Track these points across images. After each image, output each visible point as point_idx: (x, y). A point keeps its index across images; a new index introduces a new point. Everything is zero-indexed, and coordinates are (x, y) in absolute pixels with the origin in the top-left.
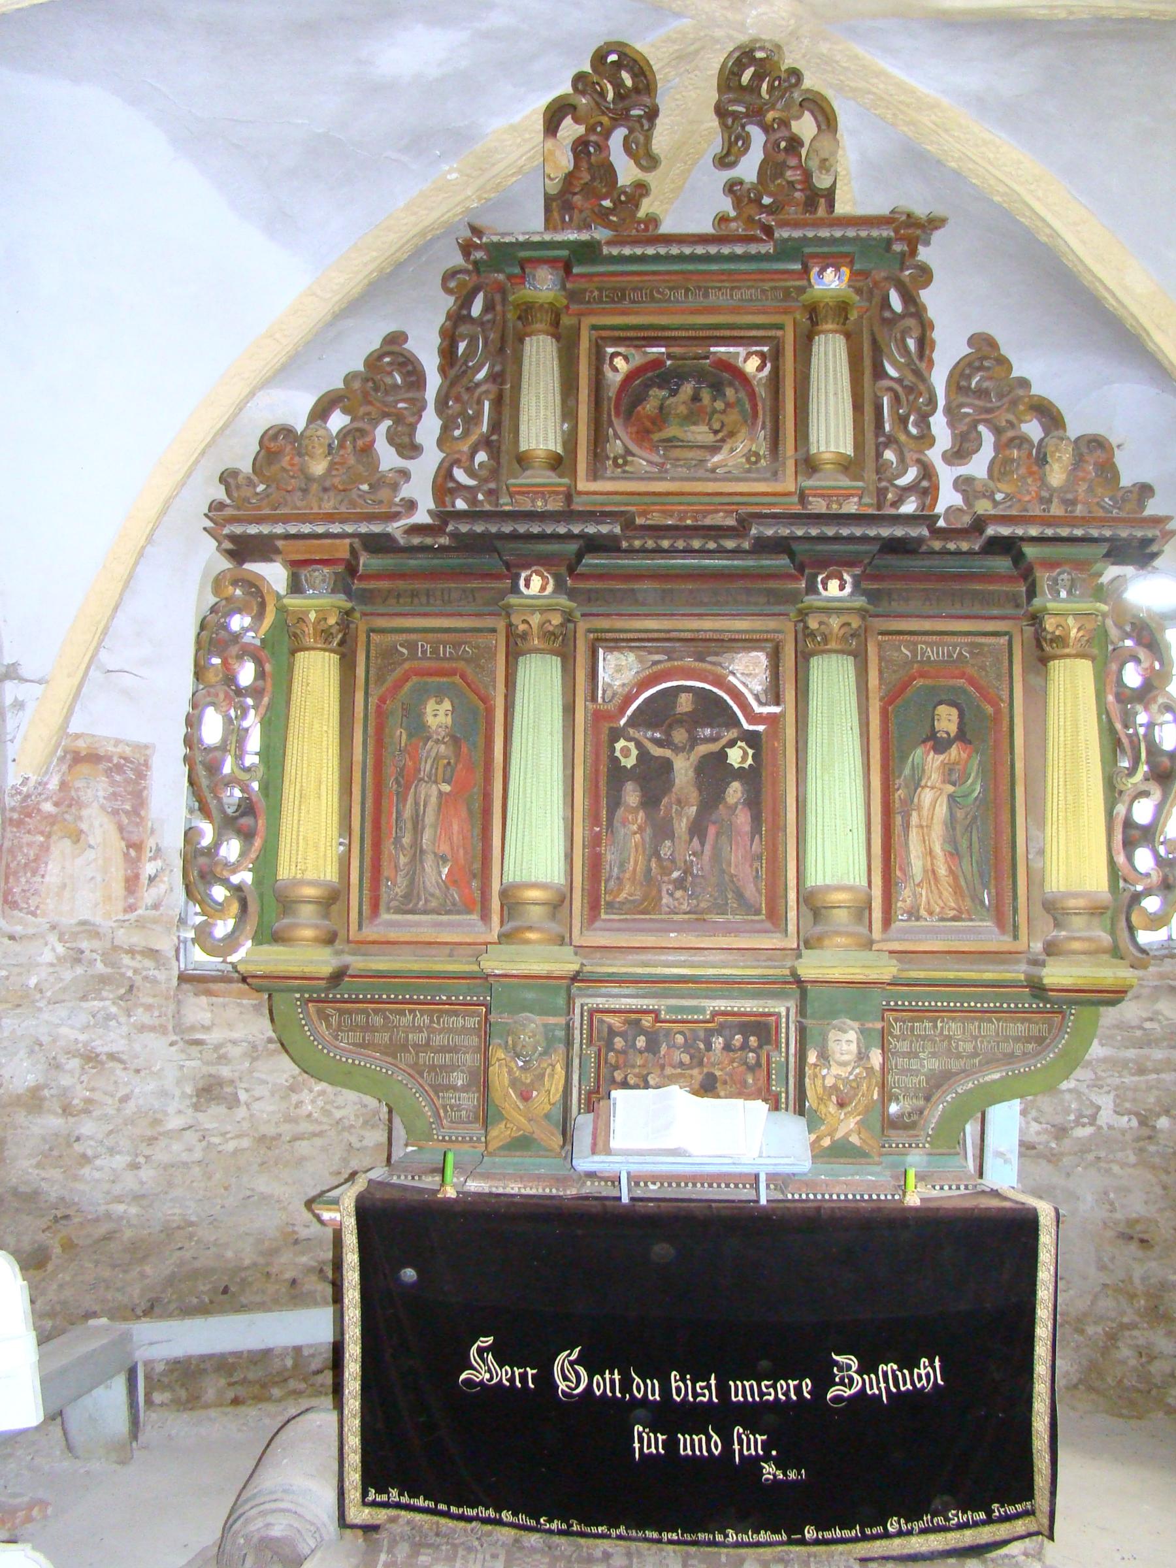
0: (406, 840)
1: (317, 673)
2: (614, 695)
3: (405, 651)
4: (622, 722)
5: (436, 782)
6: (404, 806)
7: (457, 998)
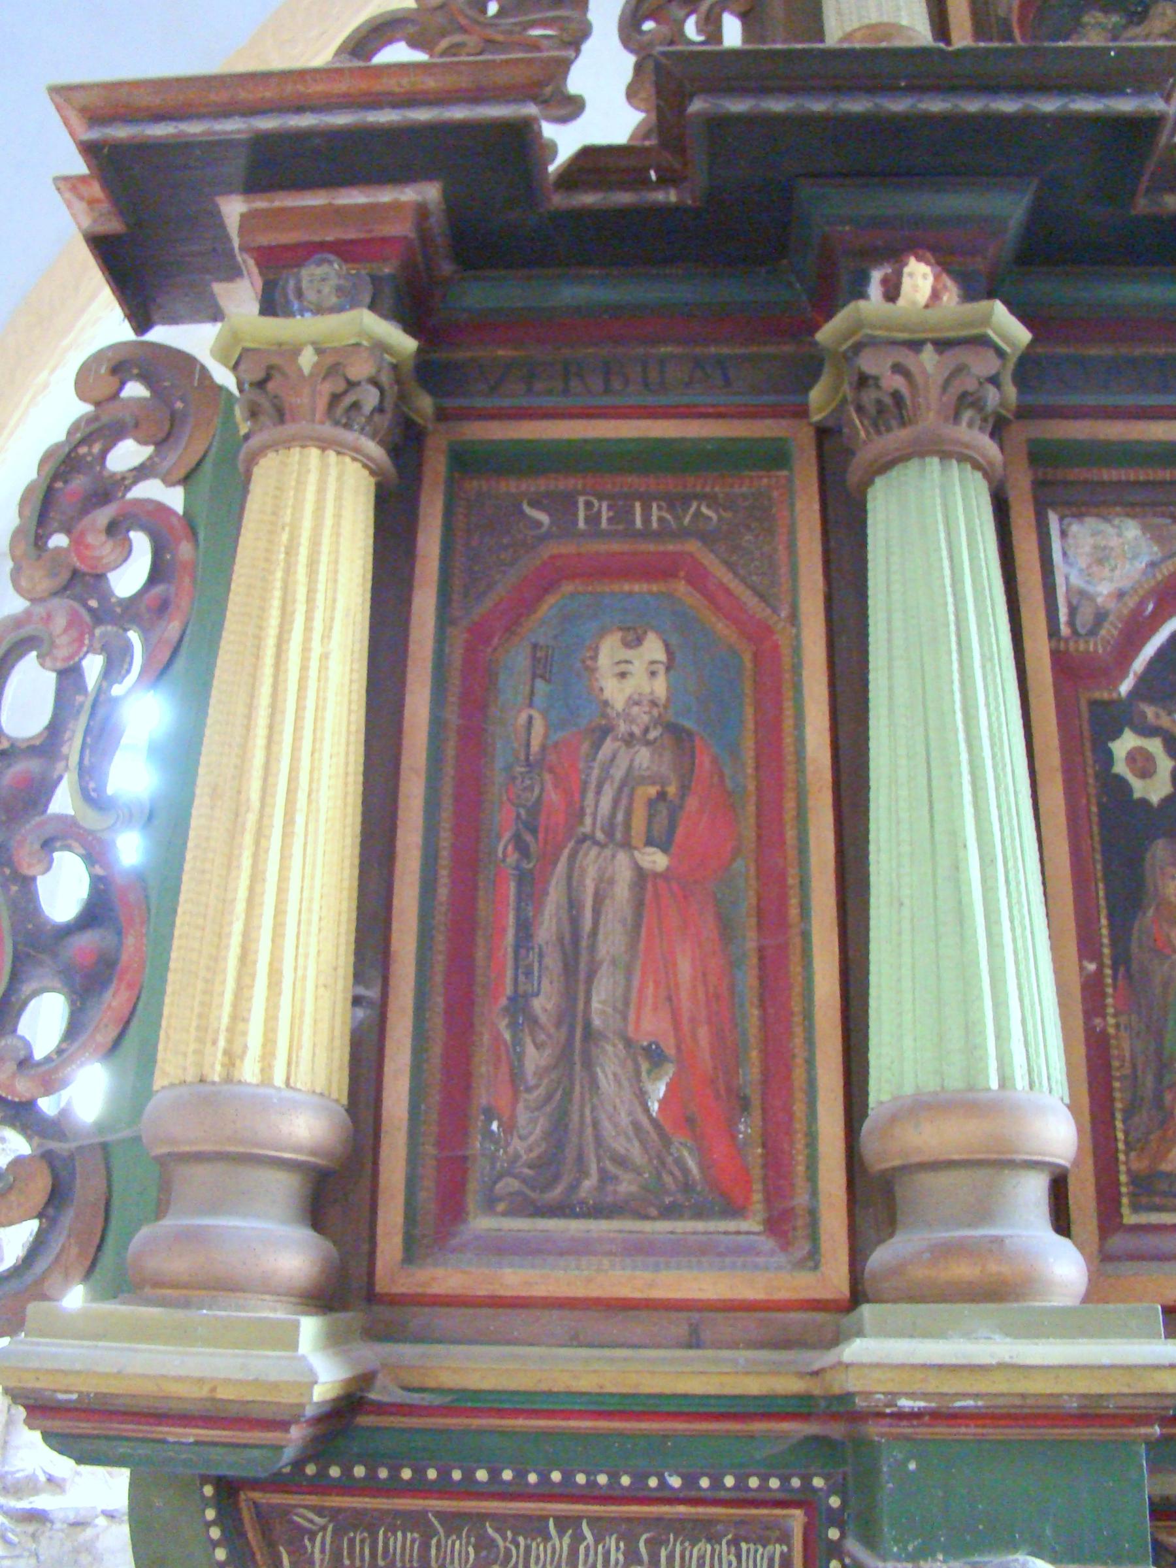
0: (544, 1004)
1: (315, 523)
2: (1100, 617)
3: (544, 518)
4: (1125, 687)
5: (627, 845)
6: (539, 907)
7: (717, 1483)
